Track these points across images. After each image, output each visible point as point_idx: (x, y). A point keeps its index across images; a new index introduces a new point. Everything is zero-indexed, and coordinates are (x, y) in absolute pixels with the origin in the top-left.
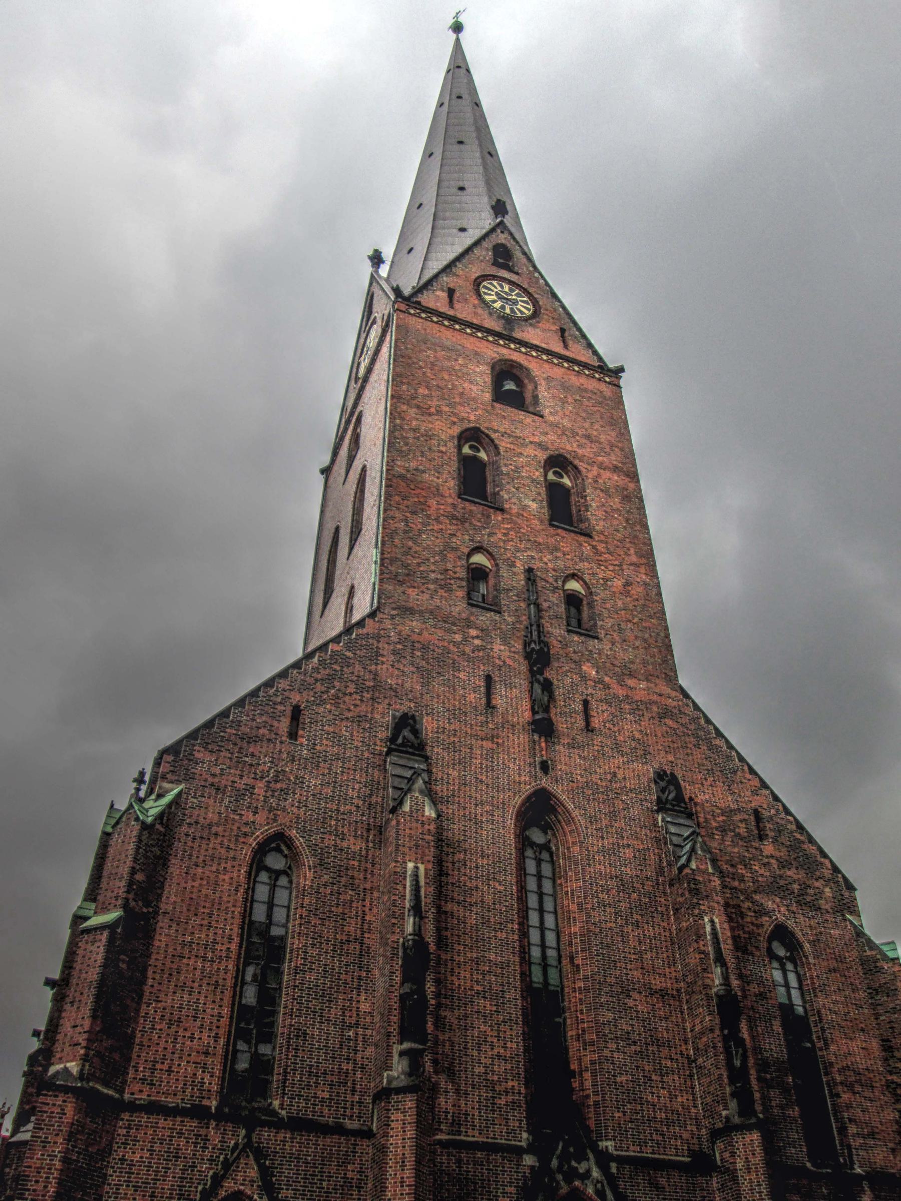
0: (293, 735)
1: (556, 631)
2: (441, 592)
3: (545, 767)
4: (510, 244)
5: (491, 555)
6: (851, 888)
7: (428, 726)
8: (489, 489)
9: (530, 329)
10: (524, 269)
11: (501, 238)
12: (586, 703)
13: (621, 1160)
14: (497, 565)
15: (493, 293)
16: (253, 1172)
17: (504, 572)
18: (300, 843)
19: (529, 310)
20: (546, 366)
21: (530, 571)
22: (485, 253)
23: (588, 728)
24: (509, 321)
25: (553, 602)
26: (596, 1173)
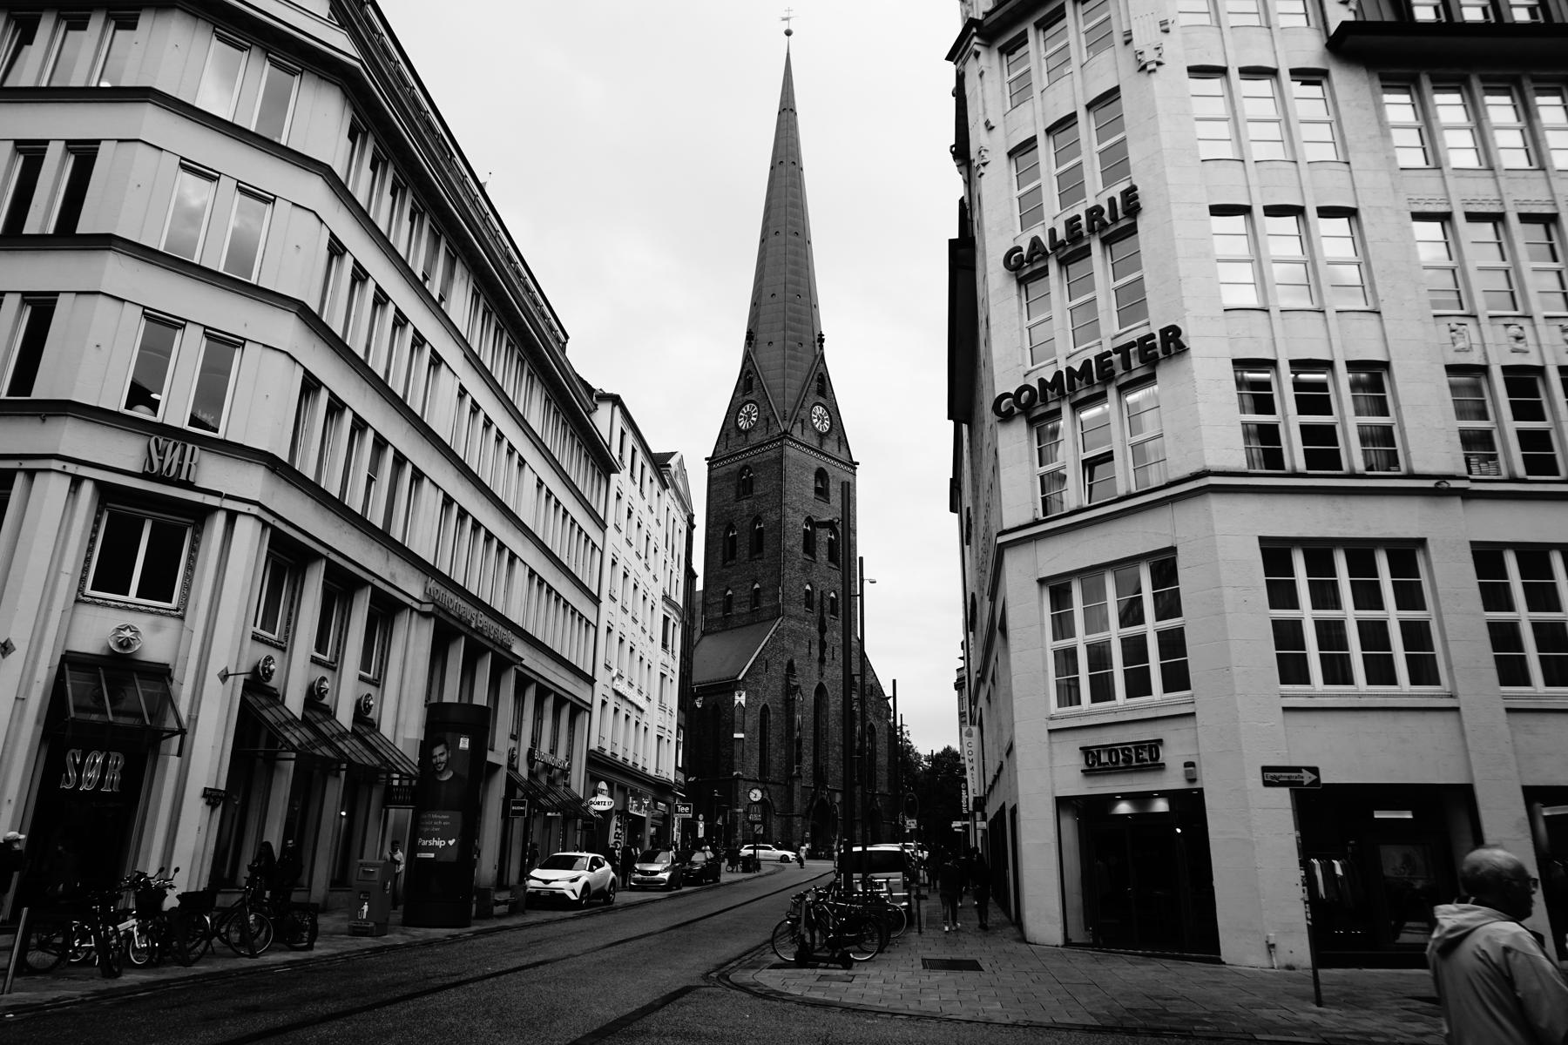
0: (766, 671)
3: (822, 675)
5: (811, 586)
8: (811, 546)
11: (821, 370)
13: (831, 790)
17: (815, 594)
20: (833, 468)
22: (815, 385)
23: (833, 658)
24: (822, 436)
25: (827, 603)
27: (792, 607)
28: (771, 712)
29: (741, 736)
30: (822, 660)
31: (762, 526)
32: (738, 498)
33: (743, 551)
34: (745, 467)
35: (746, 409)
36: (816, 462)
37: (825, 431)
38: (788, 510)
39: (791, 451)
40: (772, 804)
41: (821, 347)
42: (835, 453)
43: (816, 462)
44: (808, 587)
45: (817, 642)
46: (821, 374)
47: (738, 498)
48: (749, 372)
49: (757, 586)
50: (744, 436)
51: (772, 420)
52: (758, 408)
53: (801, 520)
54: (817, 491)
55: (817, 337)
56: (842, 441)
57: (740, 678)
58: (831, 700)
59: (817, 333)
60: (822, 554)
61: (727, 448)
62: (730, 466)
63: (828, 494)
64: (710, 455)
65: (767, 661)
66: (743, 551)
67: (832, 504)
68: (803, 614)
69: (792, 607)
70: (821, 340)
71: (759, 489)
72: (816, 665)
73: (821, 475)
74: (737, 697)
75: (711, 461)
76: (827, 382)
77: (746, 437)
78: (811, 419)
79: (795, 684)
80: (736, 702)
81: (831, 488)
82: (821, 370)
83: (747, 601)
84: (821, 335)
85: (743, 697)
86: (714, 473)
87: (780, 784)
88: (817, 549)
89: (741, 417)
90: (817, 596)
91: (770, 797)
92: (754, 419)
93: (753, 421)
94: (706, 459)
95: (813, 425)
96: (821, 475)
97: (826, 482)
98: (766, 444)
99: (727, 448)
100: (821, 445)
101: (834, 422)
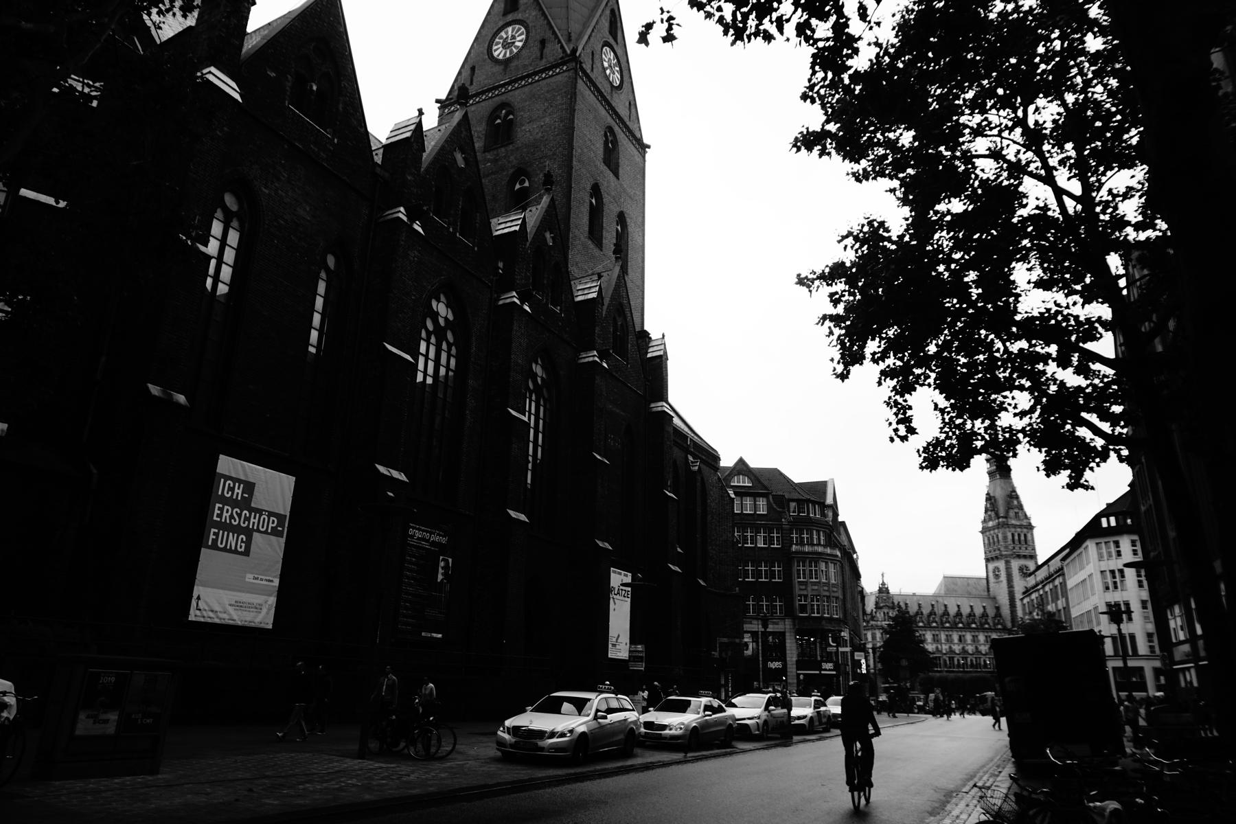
15: (607, 60)
34: (503, 105)
35: (507, 33)
52: (525, 28)
64: (443, 96)
78: (602, 60)
94: (438, 101)
95: (604, 69)
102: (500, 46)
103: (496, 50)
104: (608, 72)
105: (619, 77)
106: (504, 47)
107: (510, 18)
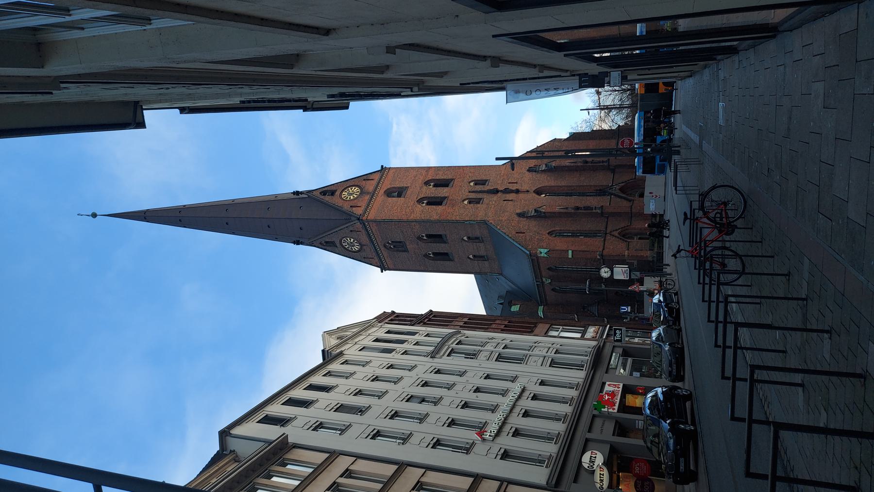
0: (524, 233)
1: (486, 188)
2: (479, 209)
3: (528, 191)
4: (321, 190)
6: (556, 139)
7: (518, 211)
9: (366, 188)
10: (333, 188)
12: (509, 183)
14: (468, 199)
15: (349, 197)
16: (615, 232)
18: (550, 231)
19: (355, 188)
21: (469, 192)
22: (327, 198)
23: (516, 183)
24: (362, 192)
25: (479, 188)
26: (615, 186)
27: (480, 214)
28: (554, 229)
29: (570, 252)
30: (517, 191)
31: (424, 235)
32: (406, 251)
33: (441, 248)
34: (385, 246)
35: (346, 245)
36: (380, 197)
37: (359, 190)
38: (412, 217)
39: (372, 215)
40: (622, 228)
41: (302, 193)
42: (374, 183)
43: (380, 197)
44: (466, 202)
45: (504, 195)
46: (321, 193)
47: (406, 251)
48: (321, 243)
49: (465, 238)
50: (364, 247)
51: (352, 229)
53: (419, 208)
54: (399, 196)
55: (295, 196)
56: (366, 177)
57: (528, 253)
58: (546, 184)
59: (293, 196)
60: (443, 192)
61: (373, 258)
62: (385, 256)
63: (402, 188)
65: (517, 233)
66: (441, 248)
67: (409, 185)
68: (484, 206)
69: (480, 214)
70: (297, 193)
71: (399, 237)
72: (521, 195)
73: (389, 193)
74: (542, 255)
75: (383, 269)
76: (326, 189)
77: (365, 245)
79: (533, 212)
80: (545, 256)
81: (398, 186)
82: (317, 194)
83: (476, 246)
84: (294, 193)
85: (542, 250)
86: (391, 267)
87: (607, 222)
88: (439, 195)
89: (351, 248)
90: (473, 196)
91: (616, 230)
92: (352, 240)
93: (354, 241)
94: (382, 272)
96: (389, 193)
97: (394, 190)
98: (368, 232)
99: (373, 258)
100: (368, 193)
101: (353, 184)
102: (353, 248)
103: (355, 249)
104: (355, 196)
105: (354, 188)
106: (354, 246)
107: (338, 245)
